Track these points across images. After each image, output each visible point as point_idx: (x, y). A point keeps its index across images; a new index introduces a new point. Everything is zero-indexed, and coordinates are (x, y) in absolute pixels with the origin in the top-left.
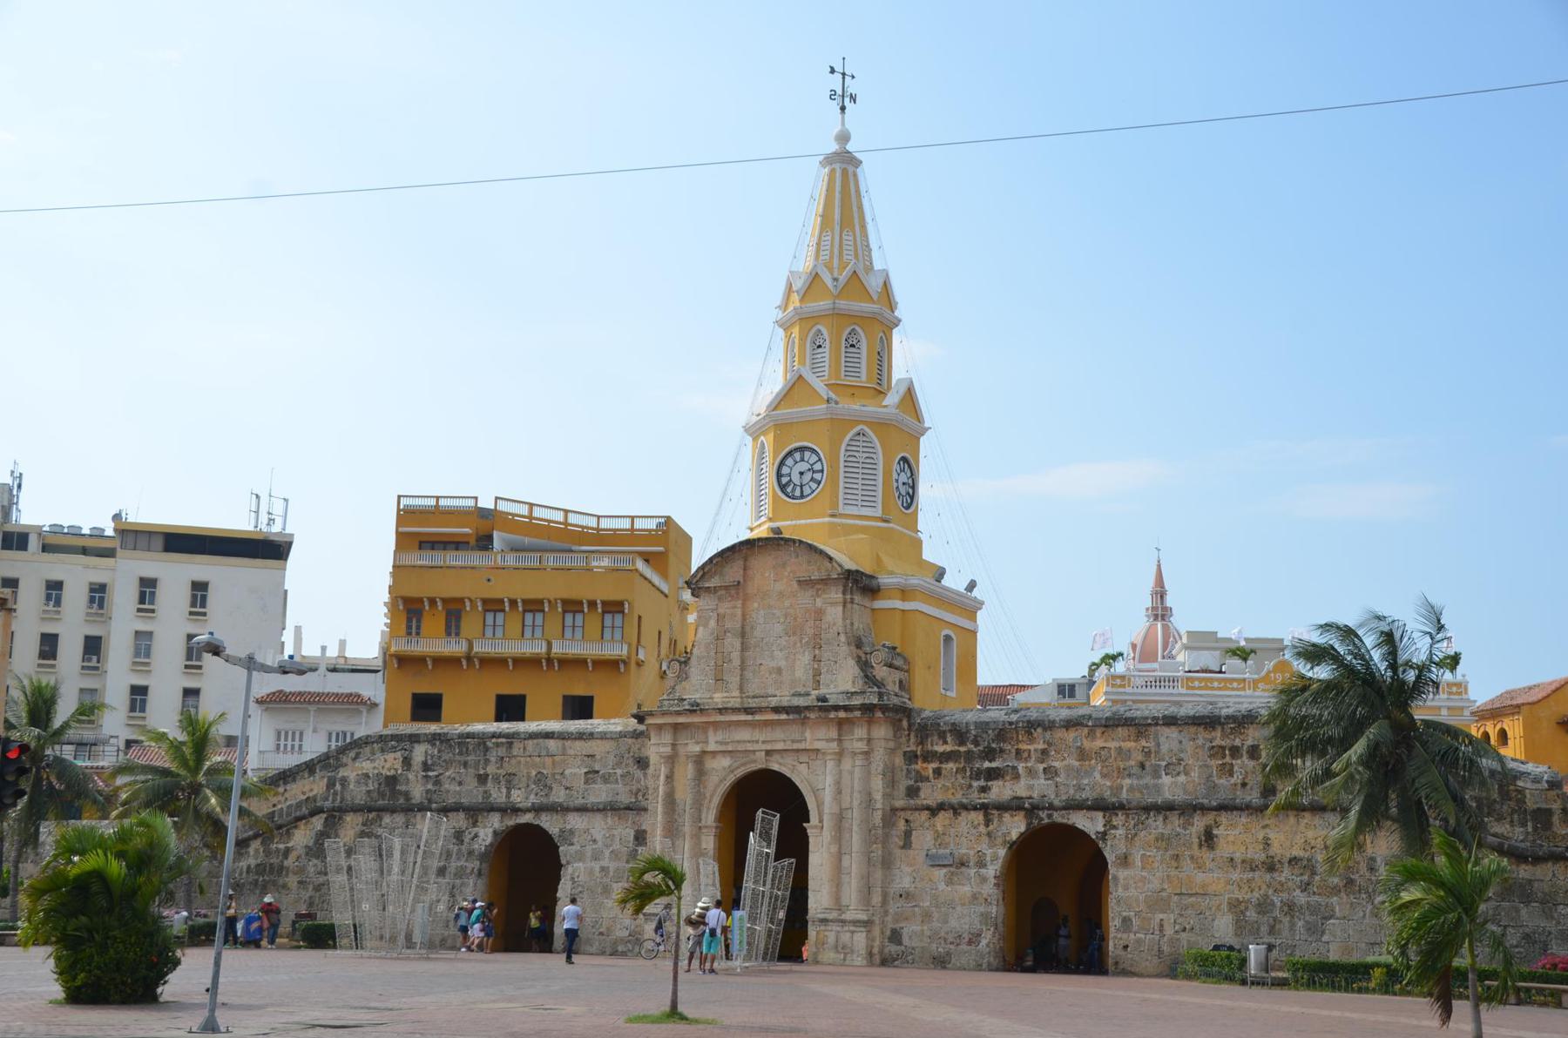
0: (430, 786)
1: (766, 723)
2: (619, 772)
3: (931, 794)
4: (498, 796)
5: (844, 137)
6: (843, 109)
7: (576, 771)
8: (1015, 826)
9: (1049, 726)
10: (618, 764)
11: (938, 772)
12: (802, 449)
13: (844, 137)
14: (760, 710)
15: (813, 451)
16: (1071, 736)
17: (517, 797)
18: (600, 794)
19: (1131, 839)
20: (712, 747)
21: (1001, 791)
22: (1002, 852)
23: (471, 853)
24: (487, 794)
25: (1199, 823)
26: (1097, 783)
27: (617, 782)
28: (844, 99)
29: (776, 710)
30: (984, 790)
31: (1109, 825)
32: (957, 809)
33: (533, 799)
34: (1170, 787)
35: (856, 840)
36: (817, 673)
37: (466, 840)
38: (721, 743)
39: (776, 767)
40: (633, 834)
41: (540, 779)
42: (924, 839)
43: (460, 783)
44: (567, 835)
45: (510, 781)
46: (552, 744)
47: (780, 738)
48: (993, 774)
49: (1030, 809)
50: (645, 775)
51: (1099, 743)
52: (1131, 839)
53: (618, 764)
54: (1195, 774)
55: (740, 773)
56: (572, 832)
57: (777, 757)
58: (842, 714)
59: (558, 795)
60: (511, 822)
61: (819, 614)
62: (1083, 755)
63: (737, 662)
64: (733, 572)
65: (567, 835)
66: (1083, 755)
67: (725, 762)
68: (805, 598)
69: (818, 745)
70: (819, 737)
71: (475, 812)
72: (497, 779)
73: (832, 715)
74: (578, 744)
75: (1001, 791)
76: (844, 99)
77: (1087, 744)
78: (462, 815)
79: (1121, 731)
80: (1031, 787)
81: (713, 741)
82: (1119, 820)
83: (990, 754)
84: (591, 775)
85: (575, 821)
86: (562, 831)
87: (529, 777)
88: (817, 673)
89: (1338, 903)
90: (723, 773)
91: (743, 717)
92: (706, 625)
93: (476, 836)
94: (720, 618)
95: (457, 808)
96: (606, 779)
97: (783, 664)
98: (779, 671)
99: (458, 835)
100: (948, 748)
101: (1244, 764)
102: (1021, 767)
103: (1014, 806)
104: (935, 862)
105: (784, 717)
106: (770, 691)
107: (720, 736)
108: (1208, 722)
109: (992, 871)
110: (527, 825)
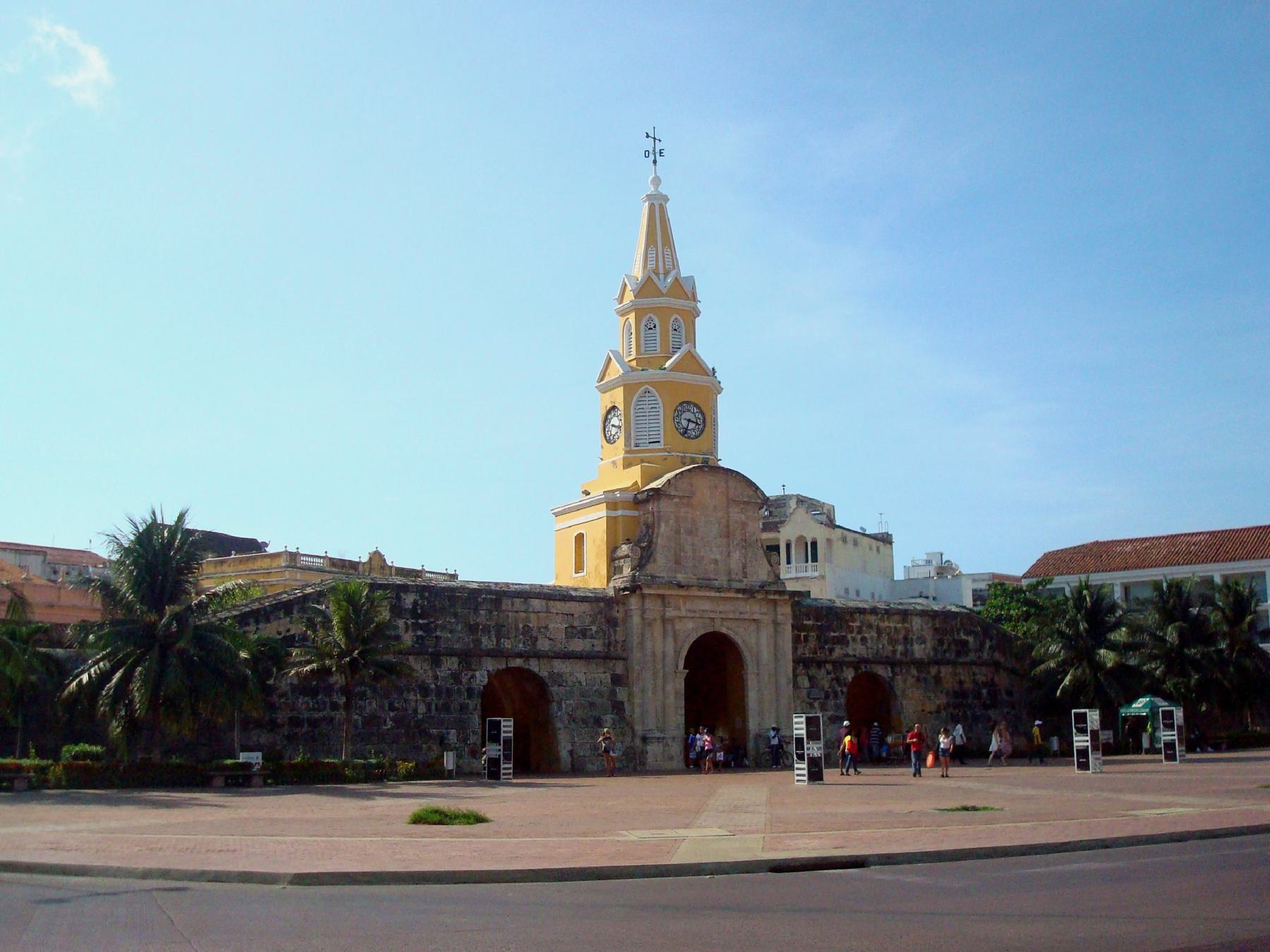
0: (420, 633)
1: (725, 599)
2: (594, 628)
4: (487, 642)
5: (657, 181)
6: (655, 162)
7: (557, 626)
8: (849, 675)
10: (593, 623)
11: (806, 638)
12: (688, 403)
13: (657, 181)
14: (729, 590)
15: (696, 405)
16: (872, 619)
17: (507, 644)
18: (579, 645)
19: (905, 681)
20: (683, 613)
21: (838, 652)
22: (845, 690)
23: (470, 692)
24: (478, 642)
25: (933, 671)
27: (592, 637)
28: (655, 155)
29: (738, 591)
30: (831, 651)
31: (894, 674)
32: (820, 664)
34: (919, 651)
36: (744, 567)
37: (464, 680)
38: (690, 611)
39: (724, 630)
40: (608, 675)
41: (527, 630)
43: (451, 632)
44: (558, 678)
46: (536, 604)
49: (858, 663)
50: (615, 631)
51: (886, 624)
52: (905, 681)
53: (593, 623)
54: (929, 645)
55: (702, 632)
56: (560, 675)
57: (728, 624)
58: (776, 597)
59: (543, 645)
61: (744, 525)
62: (879, 631)
63: (690, 554)
66: (879, 631)
67: (690, 625)
68: (736, 514)
69: (755, 617)
70: (754, 609)
71: (468, 658)
72: (486, 630)
73: (771, 597)
74: (559, 606)
75: (838, 652)
76: (655, 155)
77: (881, 624)
78: (455, 659)
79: (897, 617)
80: (854, 650)
82: (897, 670)
84: (571, 632)
85: (559, 666)
86: (551, 674)
87: (517, 629)
88: (744, 567)
89: (991, 713)
91: (713, 594)
92: (667, 522)
93: (473, 677)
94: (677, 519)
95: (451, 653)
96: (584, 634)
97: (718, 557)
98: (716, 562)
99: (456, 677)
100: (810, 622)
102: (849, 636)
105: (740, 596)
106: (712, 576)
107: (688, 606)
109: (842, 701)
110: (519, 670)
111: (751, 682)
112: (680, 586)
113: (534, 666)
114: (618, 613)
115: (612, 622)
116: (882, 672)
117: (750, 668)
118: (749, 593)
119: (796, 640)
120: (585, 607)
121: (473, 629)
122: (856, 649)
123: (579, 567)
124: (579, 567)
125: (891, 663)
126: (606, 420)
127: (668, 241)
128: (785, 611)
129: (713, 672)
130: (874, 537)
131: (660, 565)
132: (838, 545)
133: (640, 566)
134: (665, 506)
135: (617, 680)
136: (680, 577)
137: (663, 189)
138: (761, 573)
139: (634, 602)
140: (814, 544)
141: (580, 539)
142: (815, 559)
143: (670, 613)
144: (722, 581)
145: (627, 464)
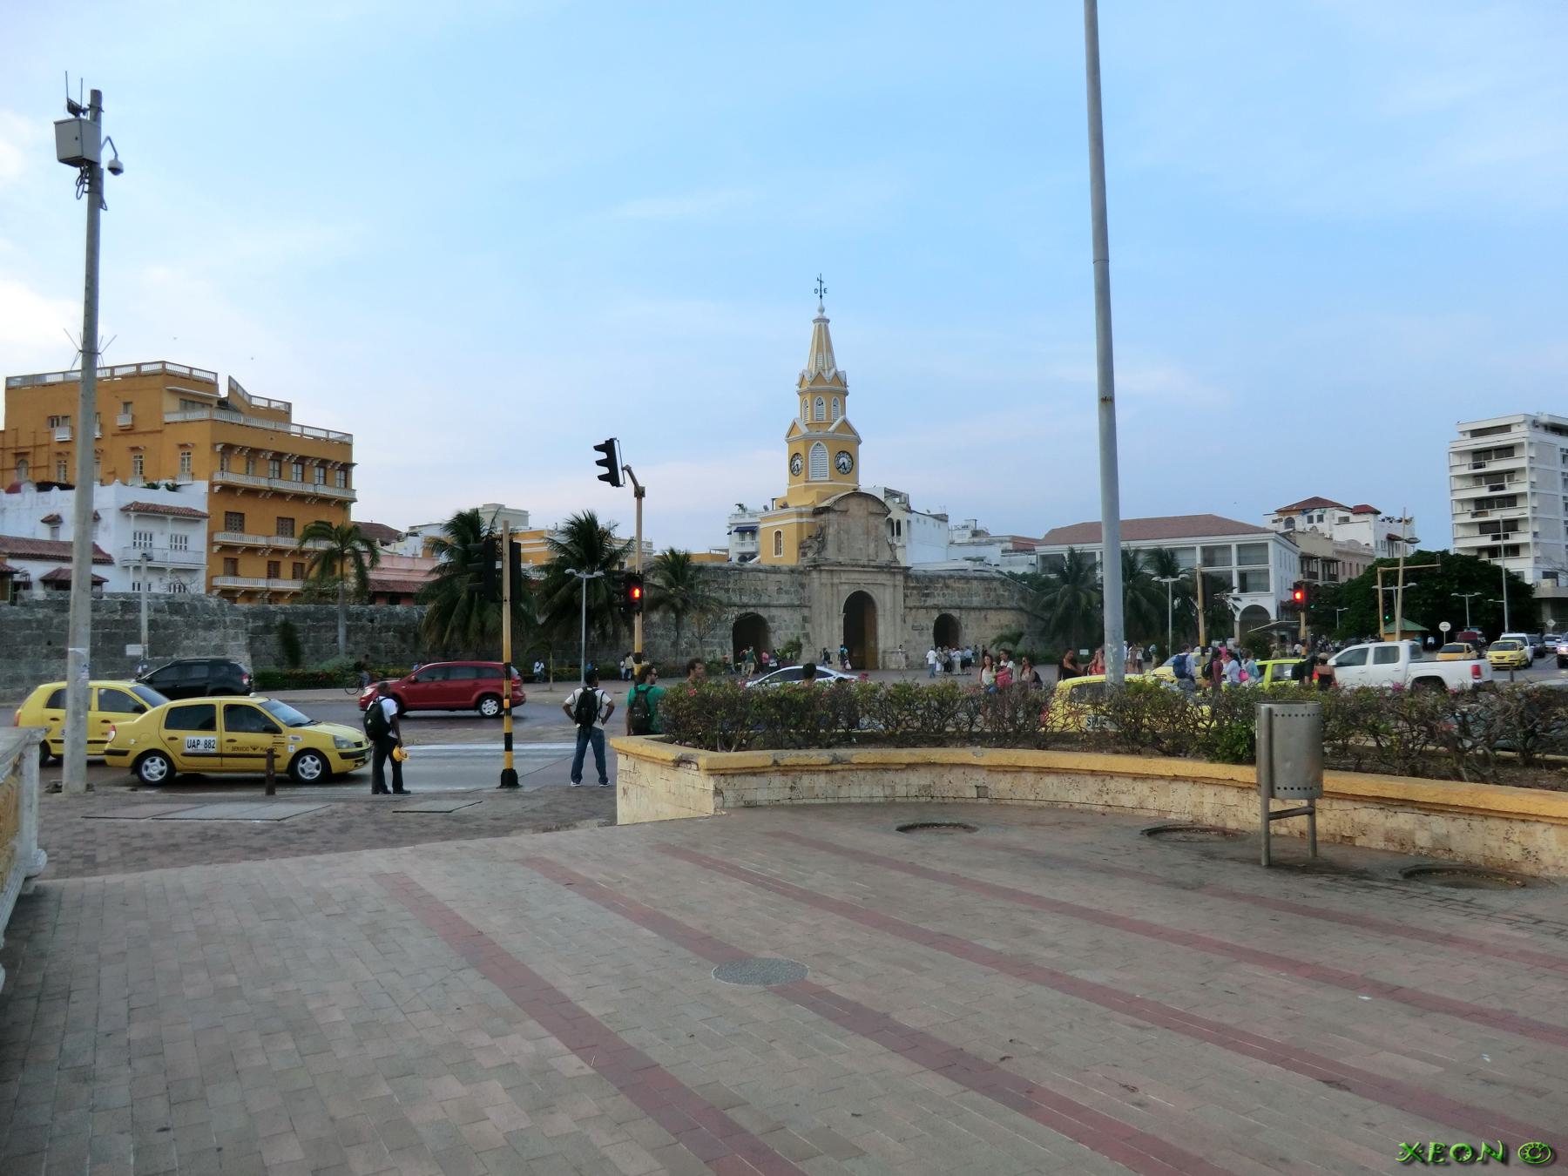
3: (910, 603)
4: (735, 599)
5: (822, 310)
7: (773, 588)
8: (936, 615)
9: (944, 578)
13: (822, 310)
17: (745, 599)
18: (784, 599)
21: (930, 602)
26: (956, 600)
33: (753, 602)
34: (976, 601)
35: (898, 619)
42: (909, 619)
44: (772, 619)
45: (741, 591)
47: (869, 578)
48: (927, 595)
59: (765, 600)
60: (743, 611)
64: (842, 507)
65: (772, 619)
68: (872, 519)
75: (930, 602)
81: (844, 578)
83: (927, 588)
85: (774, 612)
90: (846, 591)
96: (787, 592)
101: (993, 594)
103: (935, 607)
104: (914, 628)
108: (983, 579)
111: (880, 621)
112: (840, 564)
113: (762, 612)
114: (805, 580)
115: (802, 586)
116: (955, 614)
117: (880, 612)
118: (881, 569)
119: (906, 596)
120: (787, 577)
121: (727, 591)
122: (938, 600)
123: (778, 551)
124: (778, 551)
125: (959, 608)
126: (792, 461)
127: (829, 349)
128: (900, 578)
129: (859, 612)
130: (936, 517)
131: (831, 553)
132: (913, 523)
133: (819, 552)
134: (832, 516)
135: (805, 619)
136: (841, 559)
137: (826, 315)
138: (885, 558)
139: (815, 575)
140: (899, 523)
141: (778, 533)
142: (899, 533)
143: (836, 581)
144: (864, 561)
145: (807, 489)
